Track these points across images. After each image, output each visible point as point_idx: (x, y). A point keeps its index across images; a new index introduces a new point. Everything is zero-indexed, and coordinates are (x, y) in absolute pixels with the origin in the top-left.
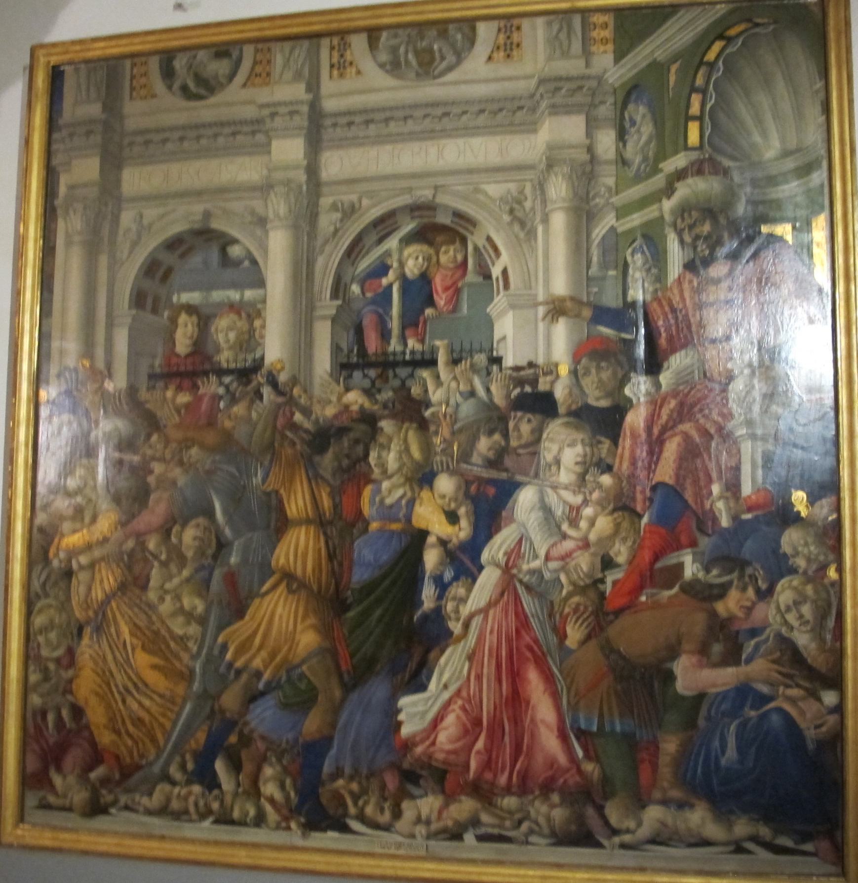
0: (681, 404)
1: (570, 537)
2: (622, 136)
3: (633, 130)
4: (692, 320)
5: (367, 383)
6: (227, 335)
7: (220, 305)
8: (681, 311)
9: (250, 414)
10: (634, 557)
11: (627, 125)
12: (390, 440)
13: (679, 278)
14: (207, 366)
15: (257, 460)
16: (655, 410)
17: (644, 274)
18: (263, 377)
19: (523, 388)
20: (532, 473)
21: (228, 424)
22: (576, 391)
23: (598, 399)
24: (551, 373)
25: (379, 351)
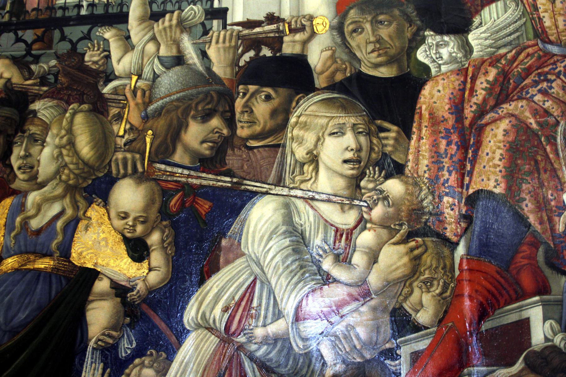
0: (504, 75)
1: (335, 281)
5: (20, 49)
10: (446, 312)
12: (46, 128)
16: (465, 82)
19: (259, 50)
20: (272, 178)
22: (341, 54)
23: (376, 66)
24: (302, 29)
25: (43, 6)
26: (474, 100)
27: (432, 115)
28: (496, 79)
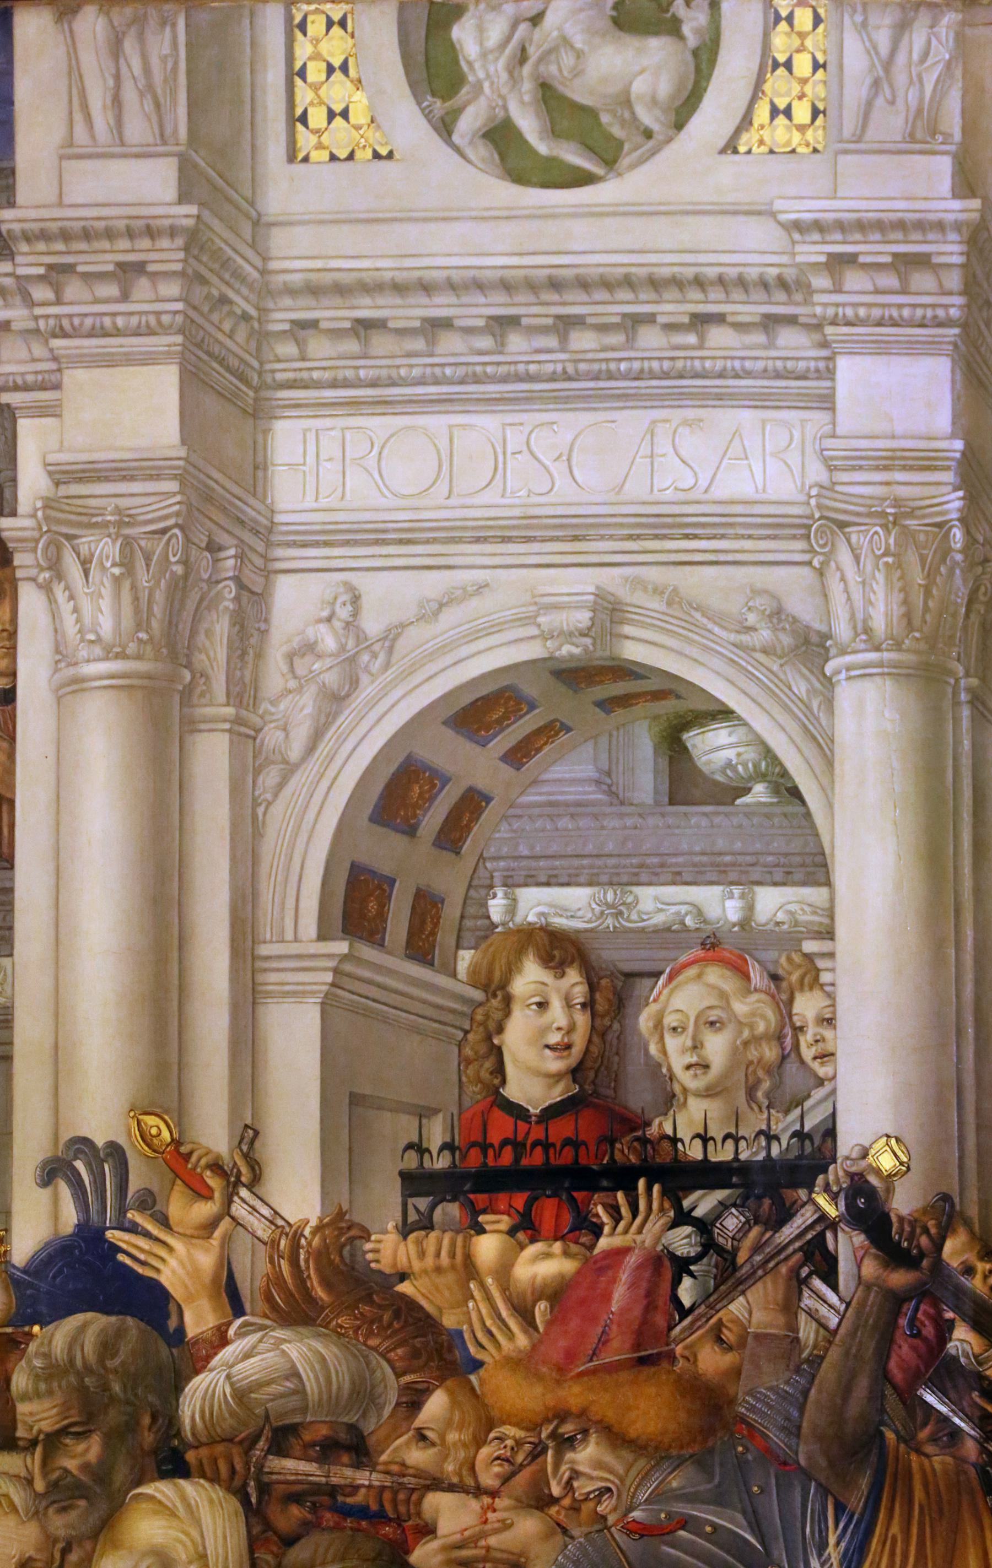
6: (697, 1046)
7: (669, 935)
9: (793, 1327)
14: (626, 1153)
15: (824, 1491)
18: (834, 1198)
21: (711, 1361)
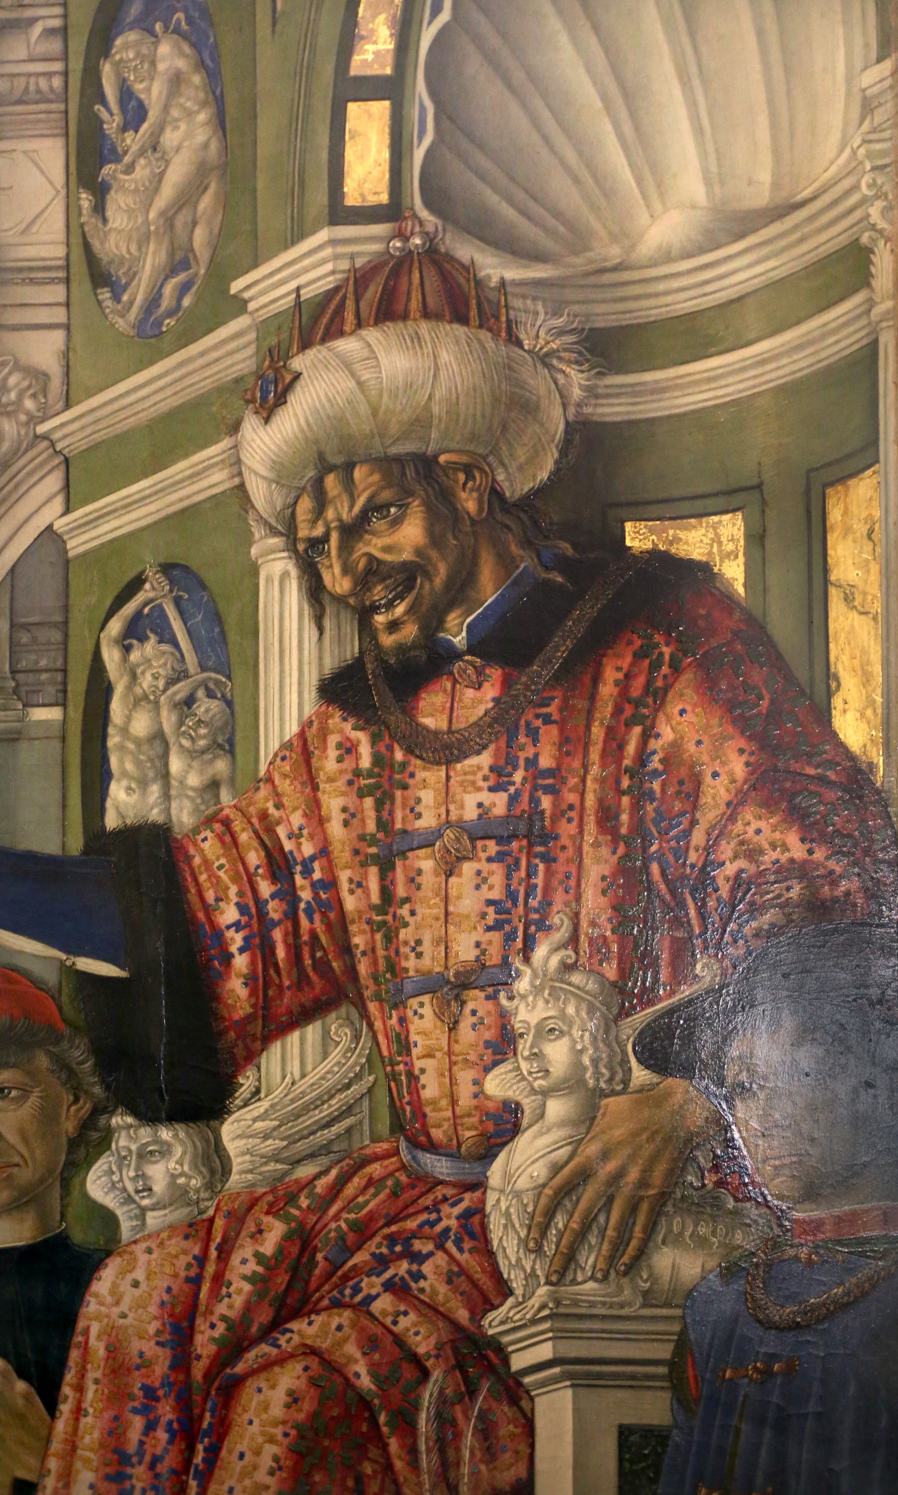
0: (303, 1239)
2: (91, 164)
3: (132, 141)
4: (350, 903)
8: (307, 872)
11: (112, 122)
13: (302, 734)
17: (168, 719)
26: (221, 1308)
27: (112, 1351)
28: (281, 1250)
